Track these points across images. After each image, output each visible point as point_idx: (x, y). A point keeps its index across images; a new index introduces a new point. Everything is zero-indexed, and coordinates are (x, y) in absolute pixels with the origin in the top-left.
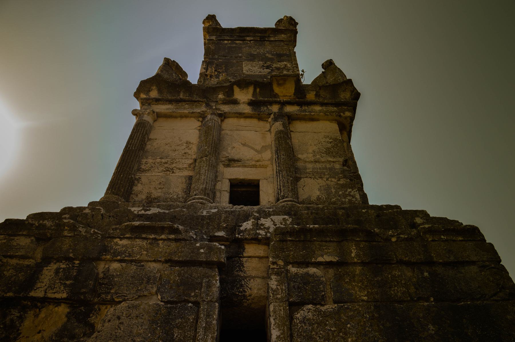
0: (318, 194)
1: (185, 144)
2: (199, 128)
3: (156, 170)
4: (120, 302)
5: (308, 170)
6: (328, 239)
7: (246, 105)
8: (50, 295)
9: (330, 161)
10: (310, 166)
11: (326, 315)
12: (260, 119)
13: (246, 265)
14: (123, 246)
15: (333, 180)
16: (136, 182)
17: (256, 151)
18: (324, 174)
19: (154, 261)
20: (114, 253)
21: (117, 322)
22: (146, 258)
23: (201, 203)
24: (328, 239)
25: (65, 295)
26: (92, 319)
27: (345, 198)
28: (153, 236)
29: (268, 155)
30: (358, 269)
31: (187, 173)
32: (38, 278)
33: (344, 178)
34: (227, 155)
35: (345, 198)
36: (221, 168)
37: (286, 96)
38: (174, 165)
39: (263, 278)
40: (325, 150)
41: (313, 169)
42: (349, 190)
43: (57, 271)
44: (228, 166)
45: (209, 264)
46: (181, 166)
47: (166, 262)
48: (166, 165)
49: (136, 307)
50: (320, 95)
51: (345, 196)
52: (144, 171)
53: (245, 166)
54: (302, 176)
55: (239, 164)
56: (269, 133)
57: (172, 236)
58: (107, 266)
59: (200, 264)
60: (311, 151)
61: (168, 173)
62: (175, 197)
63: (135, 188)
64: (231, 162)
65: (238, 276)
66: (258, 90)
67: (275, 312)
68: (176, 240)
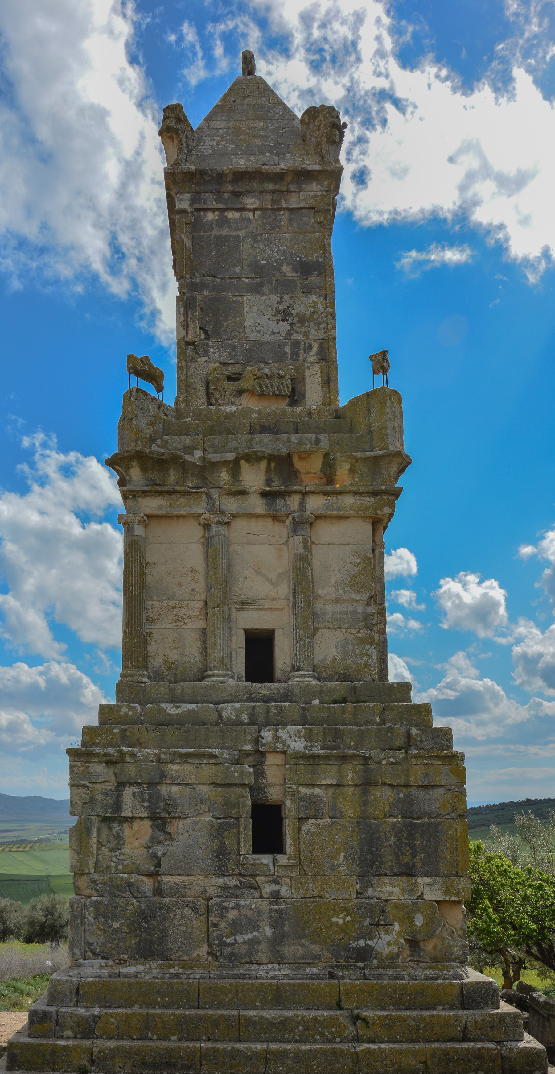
0: (334, 654)
1: (190, 573)
2: (202, 540)
3: (166, 620)
4: (186, 818)
5: (327, 616)
6: (331, 763)
7: (258, 496)
8: (136, 815)
9: (353, 600)
10: (329, 608)
11: (323, 828)
12: (275, 518)
15: (353, 631)
16: (149, 639)
17: (271, 582)
18: (344, 622)
19: (203, 784)
20: (171, 778)
21: (187, 834)
23: (222, 682)
24: (331, 763)
25: (146, 815)
26: (169, 829)
27: (361, 659)
29: (284, 589)
30: (350, 790)
31: (200, 624)
32: (122, 802)
33: (365, 627)
34: (239, 592)
35: (361, 659)
36: (235, 613)
37: (310, 473)
38: (183, 611)
39: (281, 785)
40: (350, 579)
41: (333, 614)
42: (367, 647)
43: (134, 794)
44: (241, 609)
45: (243, 785)
46: (191, 613)
47: (211, 784)
48: (175, 612)
49: (196, 823)
50: (355, 470)
51: (361, 655)
52: (154, 621)
53: (259, 609)
54: (320, 626)
55: (253, 606)
56: (285, 547)
58: (169, 789)
59: (236, 785)
60: (333, 582)
61: (179, 624)
62: (192, 660)
63: (149, 648)
64: (244, 605)
65: (262, 783)
66: (273, 465)
67: (289, 826)
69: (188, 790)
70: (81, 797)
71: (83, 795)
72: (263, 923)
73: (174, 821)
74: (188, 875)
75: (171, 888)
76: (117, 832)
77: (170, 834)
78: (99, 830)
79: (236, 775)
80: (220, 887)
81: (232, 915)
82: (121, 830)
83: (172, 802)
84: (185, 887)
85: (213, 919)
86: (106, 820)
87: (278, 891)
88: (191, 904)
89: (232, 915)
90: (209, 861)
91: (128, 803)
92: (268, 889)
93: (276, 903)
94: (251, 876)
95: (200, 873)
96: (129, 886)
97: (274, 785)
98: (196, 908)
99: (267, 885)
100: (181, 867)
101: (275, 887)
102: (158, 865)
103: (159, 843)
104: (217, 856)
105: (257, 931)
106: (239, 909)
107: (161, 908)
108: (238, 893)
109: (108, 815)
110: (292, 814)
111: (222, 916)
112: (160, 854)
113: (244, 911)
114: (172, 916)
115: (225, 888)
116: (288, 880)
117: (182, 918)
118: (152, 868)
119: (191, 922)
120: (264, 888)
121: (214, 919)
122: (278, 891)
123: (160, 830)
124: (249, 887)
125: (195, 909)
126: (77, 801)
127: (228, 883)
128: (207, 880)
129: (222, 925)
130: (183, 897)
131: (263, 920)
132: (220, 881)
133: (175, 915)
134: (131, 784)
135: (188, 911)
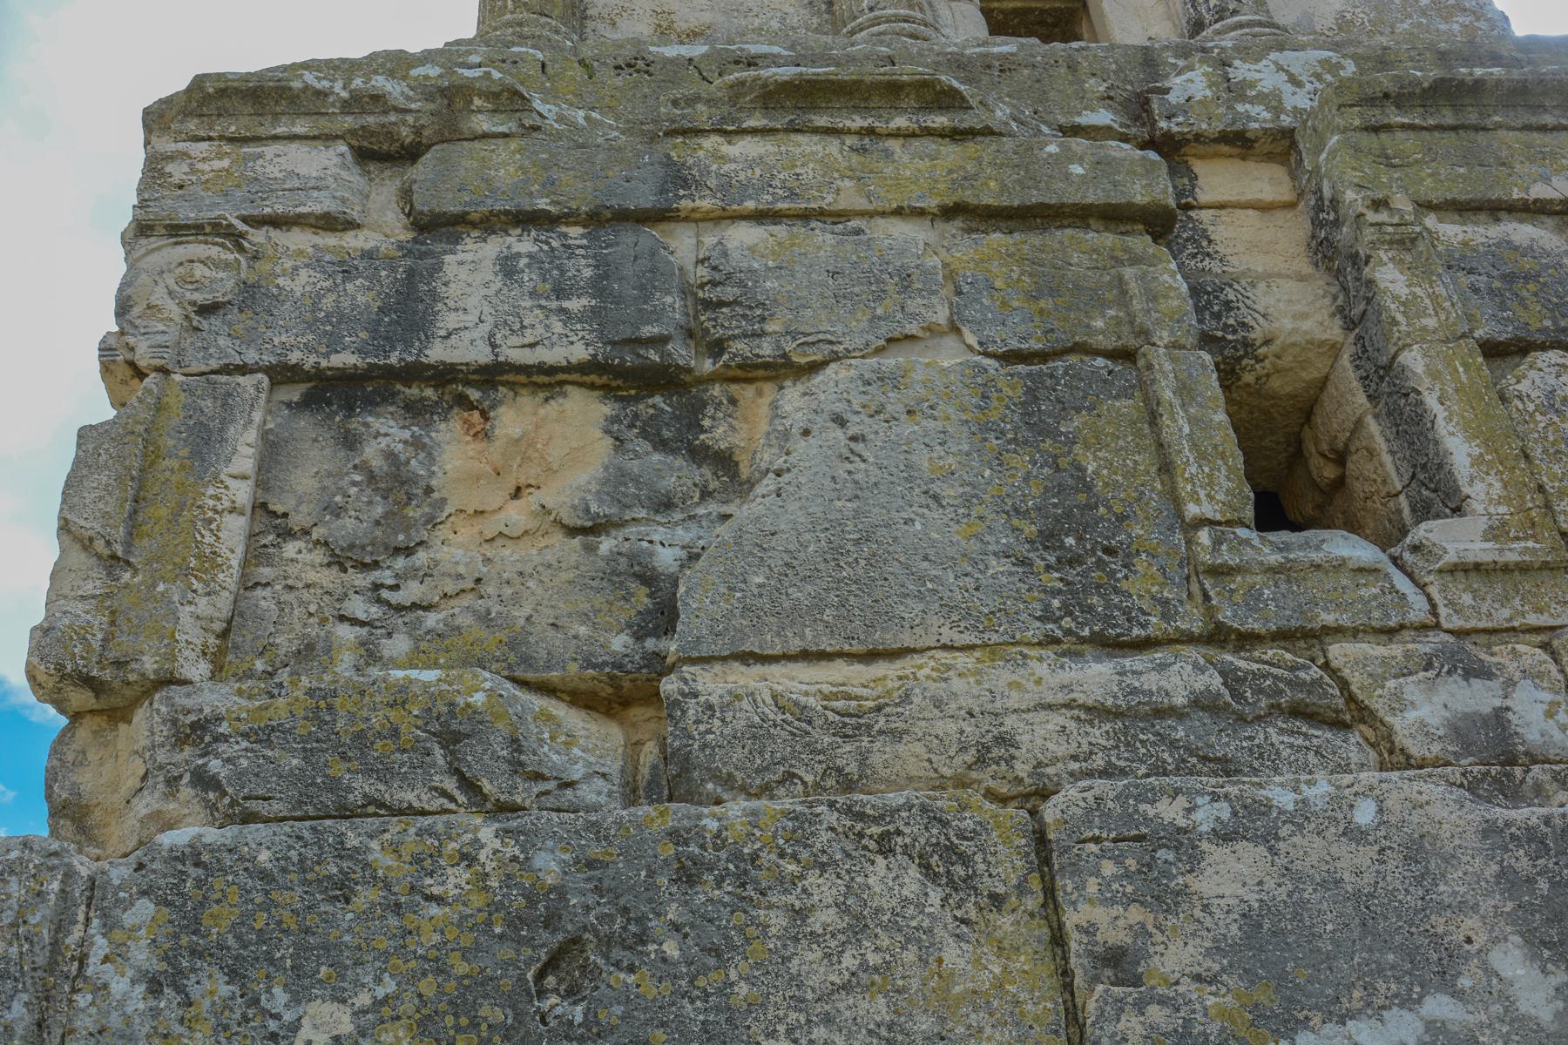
4: (815, 368)
6: (1548, 119)
13: (1217, 233)
14: (751, 164)
19: (898, 212)
21: (839, 434)
22: (862, 204)
25: (579, 353)
26: (718, 434)
28: (858, 122)
47: (949, 212)
57: (940, 120)
59: (1081, 215)
62: (775, 24)
68: (956, 135)
69: (822, 238)
70: (182, 281)
71: (199, 271)
72: (1470, 923)
73: (746, 392)
74: (871, 656)
75: (757, 734)
76: (390, 456)
77: (724, 461)
78: (272, 451)
79: (1077, 169)
80: (1098, 712)
81: (1230, 878)
82: (416, 444)
83: (729, 292)
84: (854, 723)
85: (1096, 915)
86: (332, 394)
87: (1500, 715)
88: (914, 831)
89: (1230, 878)
90: (997, 566)
91: (473, 302)
92: (1424, 710)
93: (1512, 794)
94: (1283, 637)
95: (948, 635)
96: (451, 740)
97: (1267, 276)
98: (951, 852)
99: (1411, 687)
100: (819, 605)
101: (1480, 698)
102: (664, 617)
103: (665, 504)
104: (1048, 539)
105: (1445, 980)
106: (1269, 839)
107: (688, 875)
108: (1227, 745)
109: (345, 359)
110: (1431, 323)
111: (1164, 898)
112: (666, 559)
113: (1309, 849)
114: (777, 921)
115: (1132, 716)
116: (1530, 653)
117: (858, 929)
118: (620, 643)
119: (929, 956)
120: (1399, 703)
121: (1100, 915)
122: (1500, 715)
123: (661, 445)
124: (1297, 712)
125: (947, 863)
126: (159, 297)
127: (1151, 681)
128: (1001, 676)
129: (1174, 957)
130: (848, 785)
131: (1464, 907)
132: (1097, 677)
133: (799, 914)
134: (489, 224)
135: (891, 882)
